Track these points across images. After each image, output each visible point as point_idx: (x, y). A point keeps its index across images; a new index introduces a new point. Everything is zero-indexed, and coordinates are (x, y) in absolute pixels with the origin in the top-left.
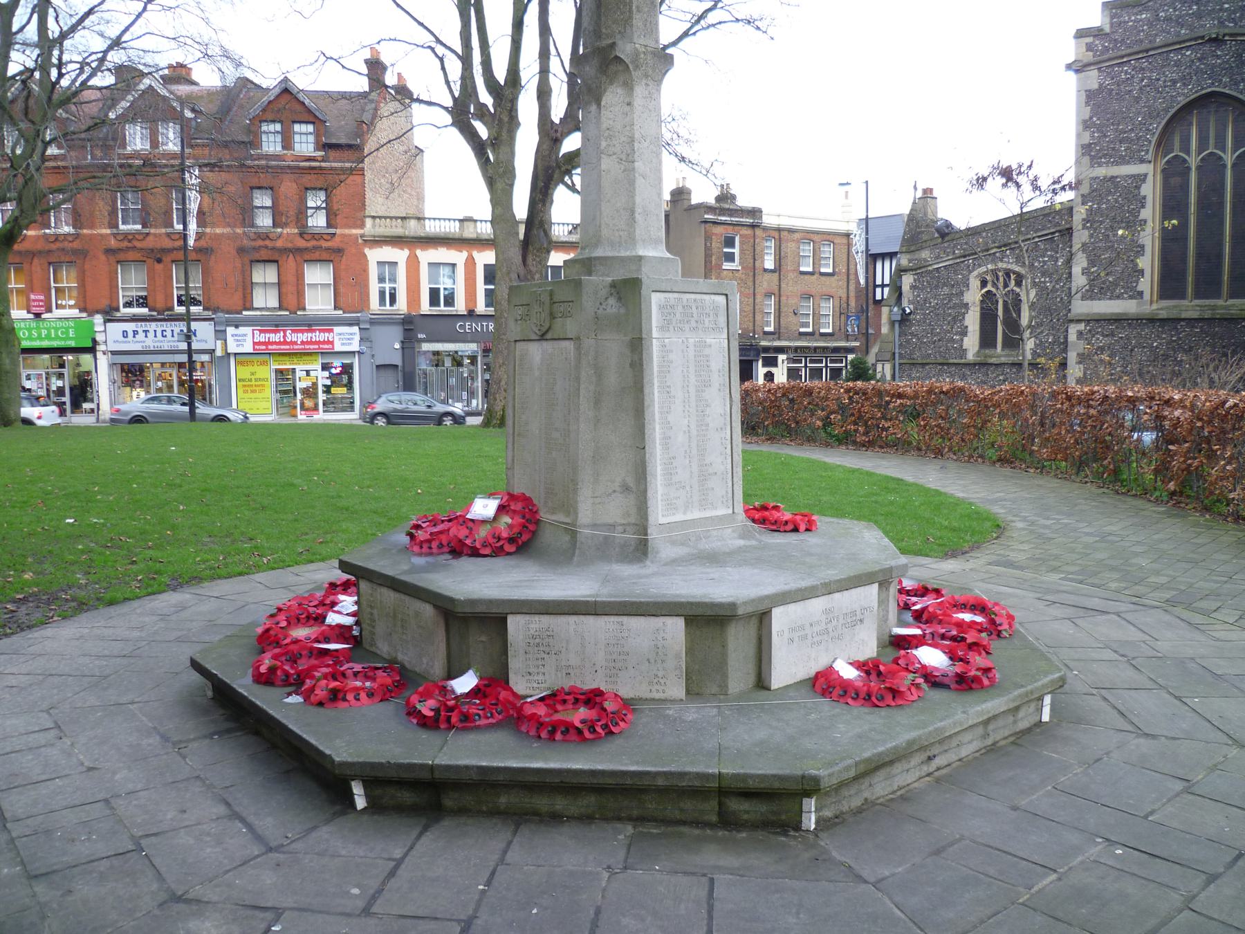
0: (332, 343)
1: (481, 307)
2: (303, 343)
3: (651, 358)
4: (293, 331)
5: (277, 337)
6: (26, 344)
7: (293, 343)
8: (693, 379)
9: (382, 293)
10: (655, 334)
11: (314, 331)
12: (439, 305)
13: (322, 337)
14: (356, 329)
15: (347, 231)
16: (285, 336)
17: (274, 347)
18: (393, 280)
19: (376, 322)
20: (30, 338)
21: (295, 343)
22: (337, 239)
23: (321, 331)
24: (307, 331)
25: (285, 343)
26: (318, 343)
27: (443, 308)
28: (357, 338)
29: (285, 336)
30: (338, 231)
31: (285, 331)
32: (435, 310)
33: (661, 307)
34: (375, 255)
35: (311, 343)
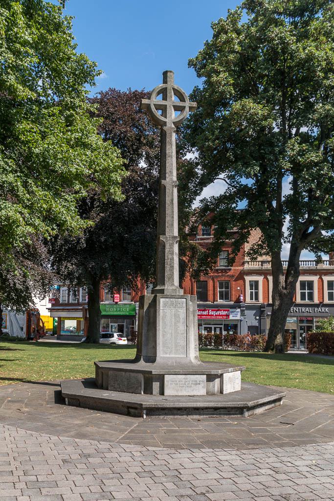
0: (229, 316)
1: (326, 301)
2: (216, 315)
3: (159, 315)
4: (212, 310)
5: (205, 313)
6: (103, 313)
7: (211, 315)
8: (173, 320)
9: (252, 293)
10: (161, 308)
11: (221, 310)
12: (253, 300)
13: (225, 313)
14: (239, 310)
15: (237, 268)
16: (209, 312)
17: (204, 317)
18: (257, 288)
19: (250, 308)
20: (105, 311)
21: (213, 315)
22: (232, 271)
23: (224, 310)
24: (218, 310)
25: (208, 315)
26: (222, 315)
27: (307, 301)
28: (239, 314)
29: (209, 312)
30: (232, 268)
31: (209, 310)
32: (303, 302)
33: (163, 302)
34: (248, 279)
35: (219, 315)
